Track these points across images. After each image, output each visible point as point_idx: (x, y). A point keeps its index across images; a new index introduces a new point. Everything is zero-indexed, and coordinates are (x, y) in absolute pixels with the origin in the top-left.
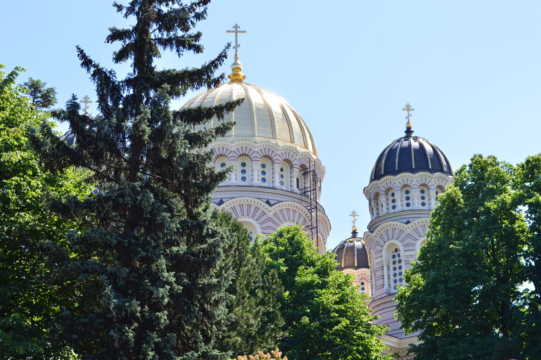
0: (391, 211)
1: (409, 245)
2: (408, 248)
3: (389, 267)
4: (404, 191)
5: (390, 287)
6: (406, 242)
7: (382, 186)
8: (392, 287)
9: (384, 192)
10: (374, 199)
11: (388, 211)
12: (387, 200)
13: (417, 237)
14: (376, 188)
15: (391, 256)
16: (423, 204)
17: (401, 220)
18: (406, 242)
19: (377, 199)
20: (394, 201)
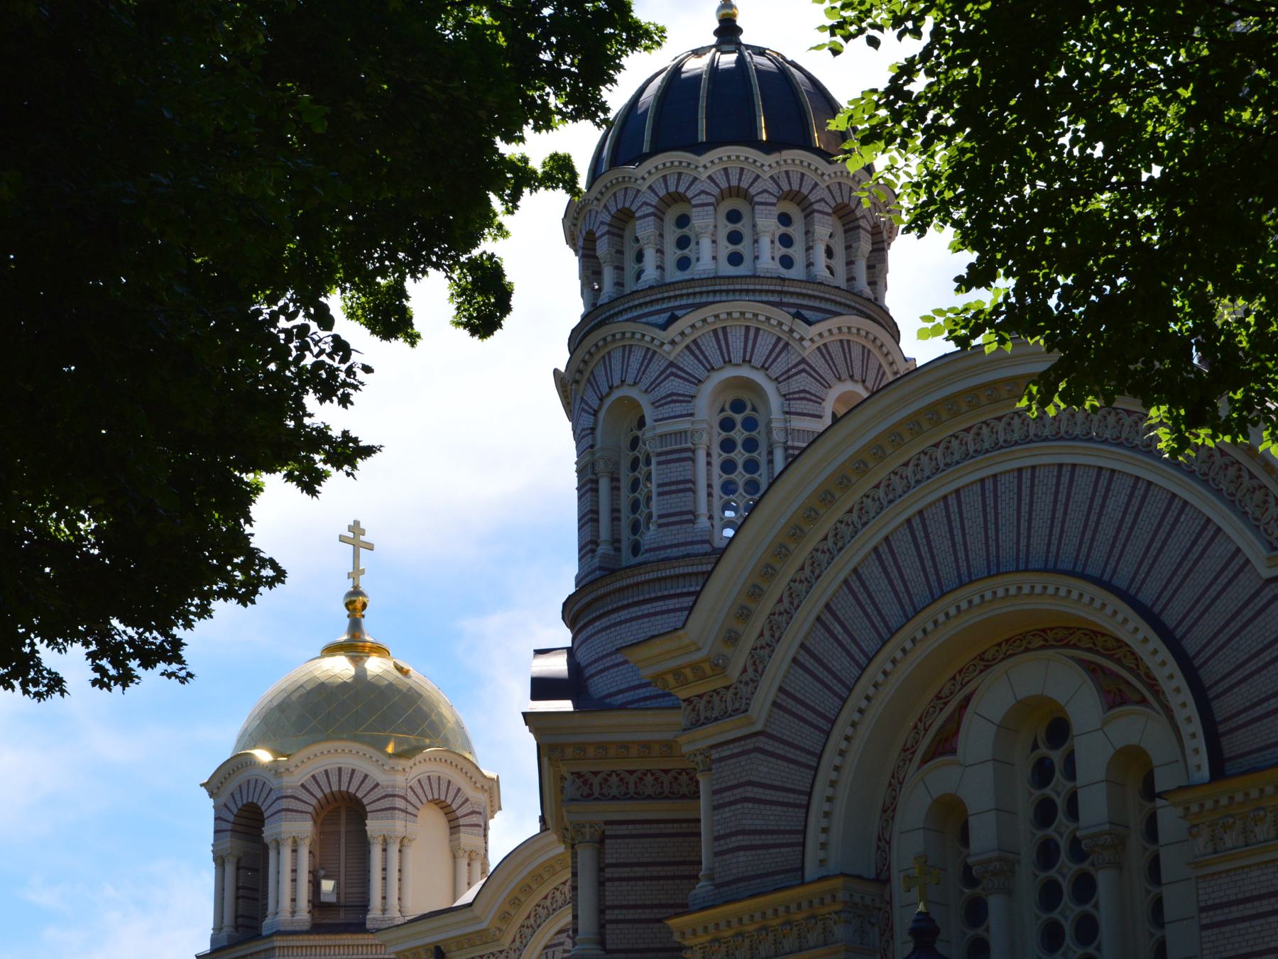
0: (674, 275)
1: (672, 398)
2: (666, 411)
3: (618, 480)
4: (730, 204)
5: (618, 550)
6: (663, 391)
7: (644, 188)
8: (625, 545)
9: (651, 210)
10: (608, 232)
11: (662, 276)
12: (661, 235)
13: (699, 372)
14: (620, 195)
15: (625, 442)
16: (735, 259)
17: (652, 319)
18: (663, 391)
19: (621, 237)
20: (683, 242)
